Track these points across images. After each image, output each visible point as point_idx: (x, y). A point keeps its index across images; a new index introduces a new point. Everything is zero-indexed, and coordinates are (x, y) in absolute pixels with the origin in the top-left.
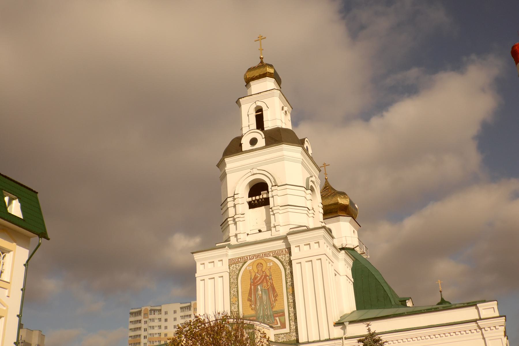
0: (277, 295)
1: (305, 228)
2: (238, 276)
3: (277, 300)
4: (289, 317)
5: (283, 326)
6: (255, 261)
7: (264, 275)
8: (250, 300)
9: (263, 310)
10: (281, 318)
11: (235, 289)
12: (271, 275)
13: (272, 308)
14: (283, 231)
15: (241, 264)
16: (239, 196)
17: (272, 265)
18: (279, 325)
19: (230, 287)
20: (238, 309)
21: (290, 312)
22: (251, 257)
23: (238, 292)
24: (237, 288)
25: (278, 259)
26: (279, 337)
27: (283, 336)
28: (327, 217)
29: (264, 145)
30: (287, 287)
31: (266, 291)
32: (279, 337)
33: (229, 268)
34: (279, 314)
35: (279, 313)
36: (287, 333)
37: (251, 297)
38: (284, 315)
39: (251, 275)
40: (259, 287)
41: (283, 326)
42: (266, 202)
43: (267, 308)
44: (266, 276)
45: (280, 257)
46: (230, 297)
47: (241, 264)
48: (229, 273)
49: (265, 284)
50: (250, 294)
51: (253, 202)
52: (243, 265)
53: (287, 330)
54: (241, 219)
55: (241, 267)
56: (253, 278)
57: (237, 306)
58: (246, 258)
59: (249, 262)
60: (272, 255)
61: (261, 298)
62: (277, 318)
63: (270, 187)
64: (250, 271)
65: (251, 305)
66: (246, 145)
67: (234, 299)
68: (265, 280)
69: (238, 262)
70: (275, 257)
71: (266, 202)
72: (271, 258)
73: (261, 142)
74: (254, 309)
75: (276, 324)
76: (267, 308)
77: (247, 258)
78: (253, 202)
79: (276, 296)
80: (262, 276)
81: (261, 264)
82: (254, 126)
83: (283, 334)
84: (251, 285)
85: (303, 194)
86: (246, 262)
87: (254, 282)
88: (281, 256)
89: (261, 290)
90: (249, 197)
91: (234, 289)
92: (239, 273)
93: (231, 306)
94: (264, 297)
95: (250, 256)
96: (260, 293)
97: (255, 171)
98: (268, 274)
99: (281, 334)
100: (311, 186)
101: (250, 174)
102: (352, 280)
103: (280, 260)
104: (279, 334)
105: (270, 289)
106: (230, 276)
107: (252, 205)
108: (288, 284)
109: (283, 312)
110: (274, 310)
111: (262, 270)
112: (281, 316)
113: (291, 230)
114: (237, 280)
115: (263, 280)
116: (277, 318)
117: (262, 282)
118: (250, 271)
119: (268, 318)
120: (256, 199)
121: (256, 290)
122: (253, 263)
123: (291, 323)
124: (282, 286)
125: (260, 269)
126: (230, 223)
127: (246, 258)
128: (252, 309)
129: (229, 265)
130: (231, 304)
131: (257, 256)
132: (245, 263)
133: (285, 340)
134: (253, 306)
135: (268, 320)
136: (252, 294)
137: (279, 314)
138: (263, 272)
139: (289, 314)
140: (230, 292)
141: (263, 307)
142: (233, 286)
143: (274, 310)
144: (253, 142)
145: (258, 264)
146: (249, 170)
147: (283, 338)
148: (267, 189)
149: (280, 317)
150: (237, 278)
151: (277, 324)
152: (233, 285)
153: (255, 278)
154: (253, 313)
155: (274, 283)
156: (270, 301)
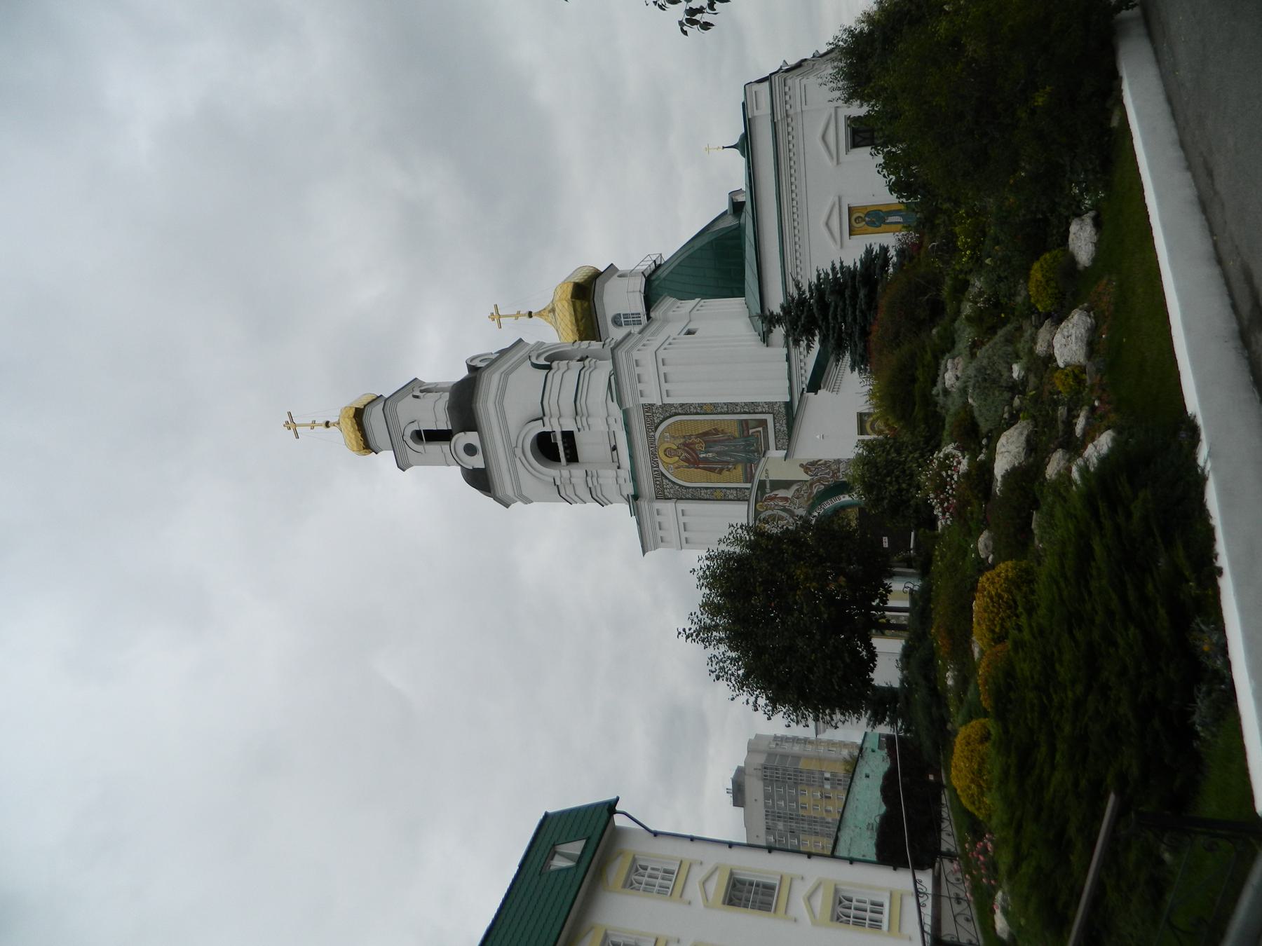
1: (612, 377)
2: (683, 486)
3: (723, 430)
4: (750, 413)
5: (763, 423)
7: (683, 447)
11: (702, 491)
12: (684, 437)
13: (735, 438)
15: (664, 481)
17: (668, 434)
18: (761, 429)
19: (700, 499)
20: (733, 488)
21: (742, 411)
22: (655, 466)
23: (707, 488)
24: (700, 488)
25: (659, 424)
26: (780, 430)
27: (777, 424)
28: (597, 336)
29: (476, 433)
30: (703, 414)
32: (780, 430)
33: (670, 499)
34: (745, 429)
35: (743, 427)
36: (774, 418)
37: (716, 468)
38: (746, 421)
40: (702, 456)
41: (763, 423)
42: (569, 437)
43: (734, 446)
44: (685, 444)
45: (656, 421)
46: (714, 500)
47: (664, 481)
48: (678, 499)
50: (712, 470)
51: (568, 457)
52: (667, 478)
53: (769, 418)
55: (670, 480)
56: (687, 464)
57: (728, 491)
58: (656, 473)
60: (652, 433)
61: (719, 453)
62: (751, 431)
64: (677, 468)
66: (477, 462)
68: (692, 446)
69: (662, 485)
70: (656, 428)
71: (569, 437)
72: (657, 434)
73: (472, 438)
74: (735, 464)
75: (759, 434)
76: (734, 446)
77: (655, 471)
78: (568, 457)
79: (716, 431)
80: (684, 450)
81: (665, 451)
82: (445, 446)
83: (775, 424)
84: (696, 468)
85: (559, 373)
86: (662, 473)
88: (655, 418)
89: (706, 452)
91: (703, 494)
92: (678, 485)
94: (717, 448)
95: (652, 466)
96: (710, 454)
97: (519, 451)
98: (682, 441)
99: (775, 427)
100: (546, 359)
101: (523, 458)
102: (698, 300)
103: (662, 422)
104: (775, 429)
105: (707, 438)
106: (682, 499)
108: (699, 411)
109: (741, 421)
110: (737, 435)
111: (675, 450)
114: (689, 488)
115: (691, 449)
116: (751, 431)
117: (693, 450)
118: (677, 468)
119: (748, 445)
121: (706, 460)
122: (663, 462)
123: (760, 410)
124: (701, 420)
127: (656, 473)
128: (735, 468)
129: (666, 499)
131: (653, 455)
132: (663, 474)
133: (784, 421)
134: (731, 466)
135: (753, 445)
136: (710, 467)
138: (678, 448)
139: (745, 413)
143: (737, 435)
144: (470, 449)
145: (666, 455)
146: (517, 460)
147: (781, 425)
148: (549, 433)
149: (750, 427)
151: (760, 432)
152: (696, 496)
153: (686, 460)
154: (740, 468)
155: (697, 433)
156: (723, 440)
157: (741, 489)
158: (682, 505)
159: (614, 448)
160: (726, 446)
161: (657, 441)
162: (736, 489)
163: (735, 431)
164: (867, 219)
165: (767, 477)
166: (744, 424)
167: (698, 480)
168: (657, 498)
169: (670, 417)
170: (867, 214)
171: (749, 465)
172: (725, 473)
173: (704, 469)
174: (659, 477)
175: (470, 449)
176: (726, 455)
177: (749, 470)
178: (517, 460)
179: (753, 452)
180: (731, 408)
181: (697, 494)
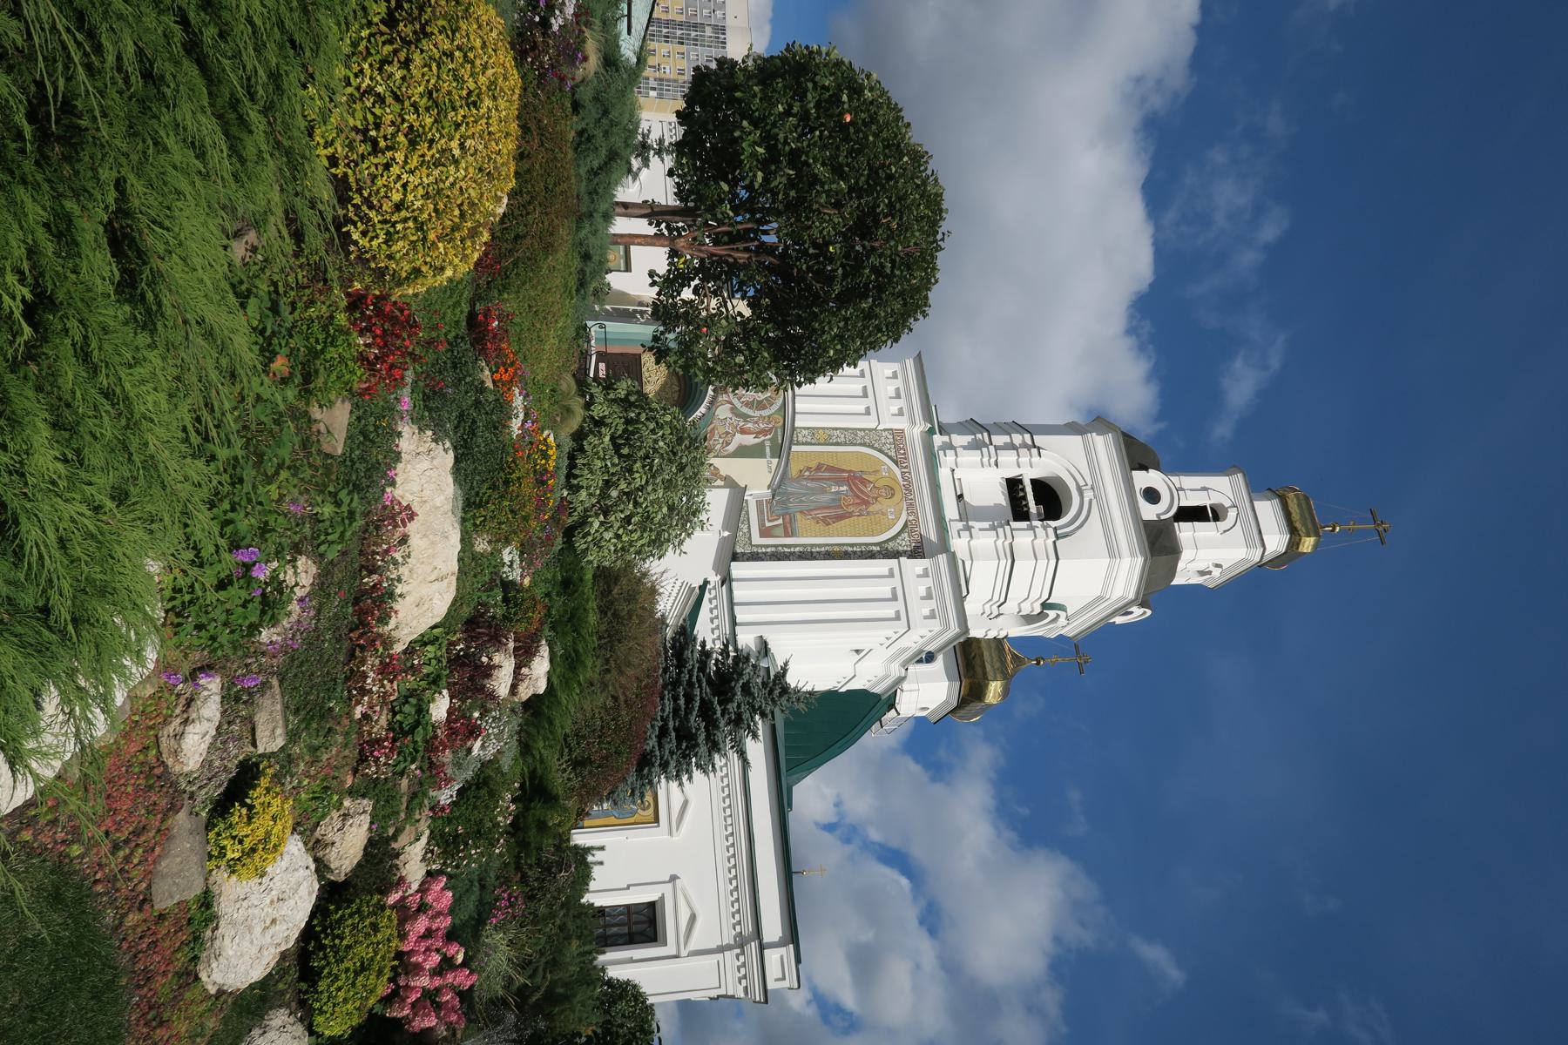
0: (828, 524)
8: (819, 468)
10: (780, 531)
12: (868, 513)
13: (801, 512)
14: (958, 544)
16: (1036, 459)
24: (845, 444)
31: (837, 501)
37: (825, 471)
38: (787, 535)
39: (870, 473)
40: (845, 488)
42: (1020, 513)
44: (867, 503)
52: (890, 458)
54: (985, 460)
55: (886, 455)
61: (823, 491)
62: (780, 521)
63: (1053, 524)
65: (809, 469)
66: (1143, 479)
67: (822, 436)
69: (897, 449)
70: (905, 525)
81: (893, 495)
87: (855, 480)
89: (838, 493)
90: (1033, 481)
92: (875, 449)
94: (825, 498)
103: (899, 534)
105: (840, 512)
107: (1013, 485)
110: (799, 516)
113: (960, 563)
121: (839, 482)
122: (894, 479)
132: (896, 463)
138: (876, 499)
141: (805, 495)
142: (849, 436)
143: (799, 516)
150: (864, 445)
153: (865, 482)
159: (960, 497)
163: (802, 522)
165: (769, 463)
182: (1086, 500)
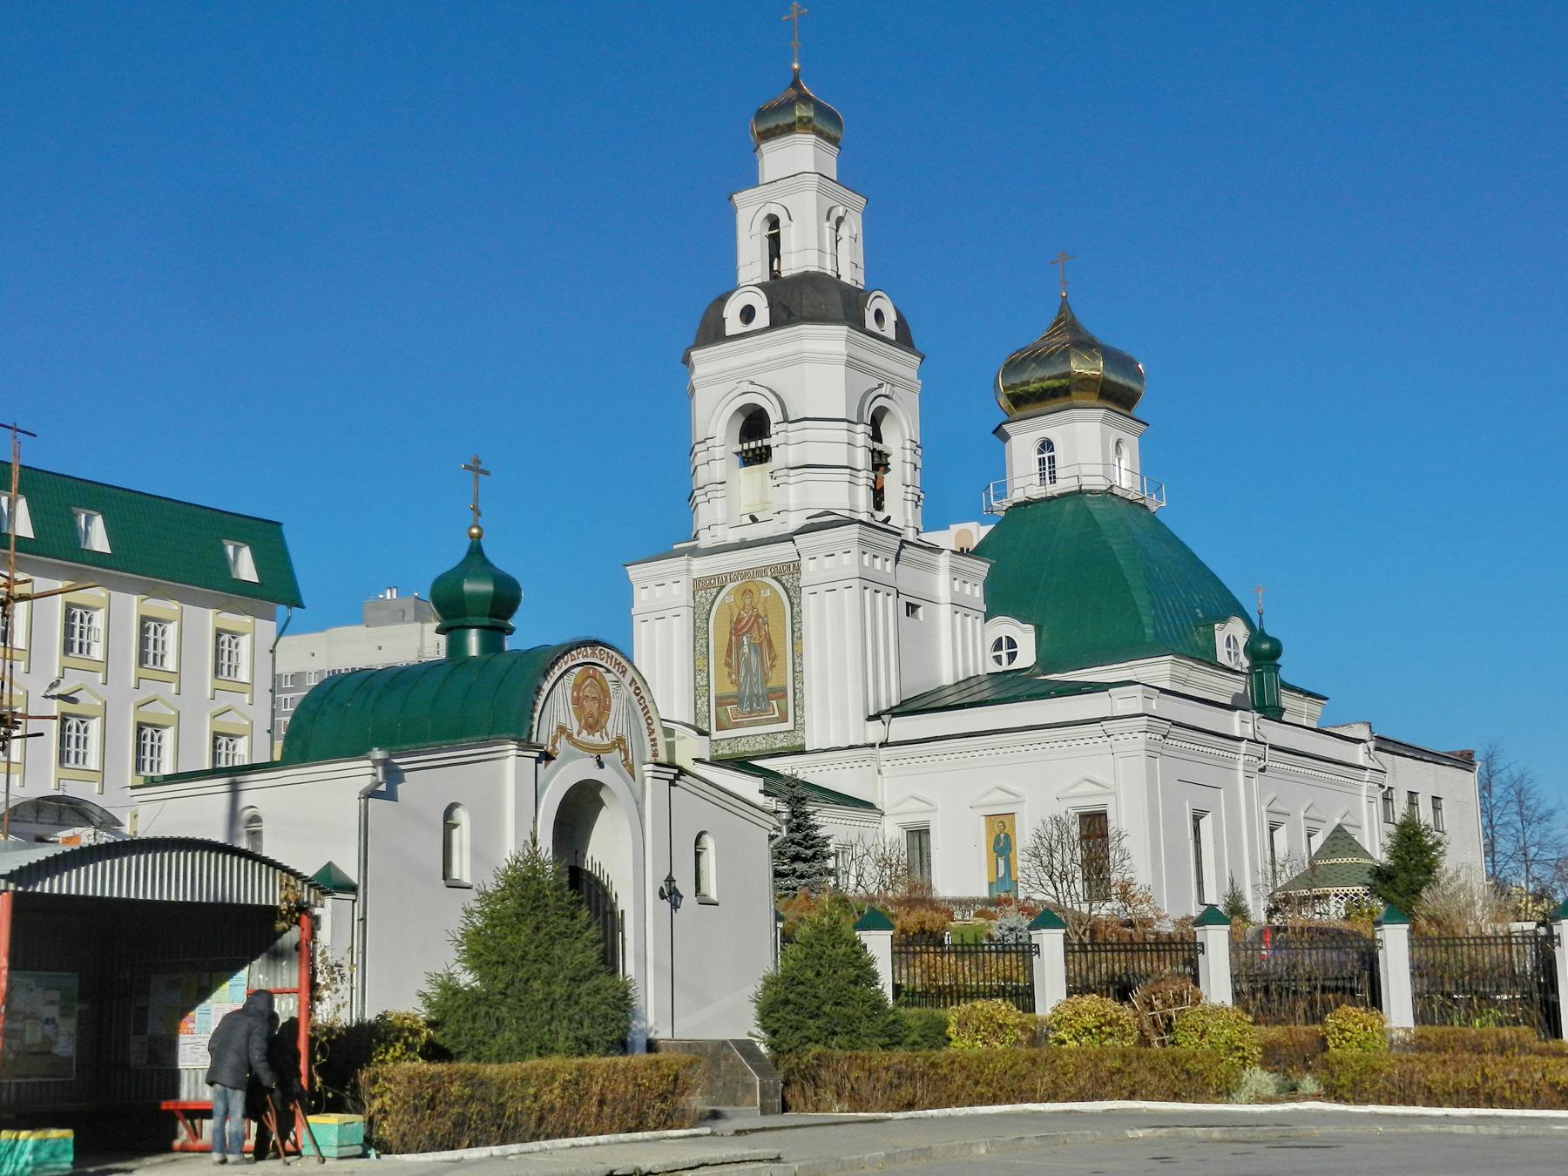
2: (709, 615)
4: (795, 700)
6: (740, 585)
8: (729, 665)
9: (751, 685)
12: (766, 616)
13: (766, 681)
16: (717, 442)
18: (777, 715)
19: (695, 637)
20: (709, 681)
24: (708, 638)
25: (780, 582)
27: (782, 735)
31: (757, 648)
34: (777, 694)
36: (789, 732)
39: (732, 615)
40: (745, 639)
43: (757, 680)
44: (758, 616)
48: (694, 608)
49: (755, 634)
52: (718, 593)
53: (789, 726)
54: (719, 494)
55: (716, 597)
59: (730, 586)
61: (748, 661)
62: (774, 702)
65: (730, 675)
66: (733, 324)
67: (701, 663)
71: (763, 456)
73: (762, 318)
76: (757, 680)
79: (773, 659)
81: (750, 591)
84: (731, 633)
87: (737, 629)
88: (787, 577)
89: (749, 645)
93: (695, 676)
94: (754, 660)
95: (731, 573)
96: (747, 651)
97: (747, 387)
98: (762, 614)
99: (780, 732)
103: (783, 585)
105: (765, 644)
106: (695, 613)
109: (784, 690)
110: (770, 685)
112: (780, 697)
114: (708, 623)
119: (758, 700)
120: (750, 449)
121: (740, 644)
125: (748, 601)
126: (698, 500)
130: (695, 670)
132: (723, 587)
137: (777, 694)
139: (795, 694)
140: (695, 647)
142: (701, 634)
143: (770, 685)
144: (748, 314)
146: (733, 384)
147: (781, 741)
150: (708, 619)
151: (774, 713)
152: (699, 631)
153: (739, 620)
154: (733, 689)
157: (709, 691)
158: (686, 614)
160: (757, 672)
161: (760, 579)
162: (708, 685)
164: (1002, 836)
166: (780, 693)
167: (717, 638)
168: (695, 580)
169: (789, 597)
170: (1007, 836)
171: (736, 701)
172: (726, 670)
173: (731, 640)
174: (718, 583)
175: (748, 314)
176: (746, 674)
177: (730, 700)
178: (733, 384)
179: (751, 706)
180: (797, 674)
181: (701, 634)
182: (751, 388)
